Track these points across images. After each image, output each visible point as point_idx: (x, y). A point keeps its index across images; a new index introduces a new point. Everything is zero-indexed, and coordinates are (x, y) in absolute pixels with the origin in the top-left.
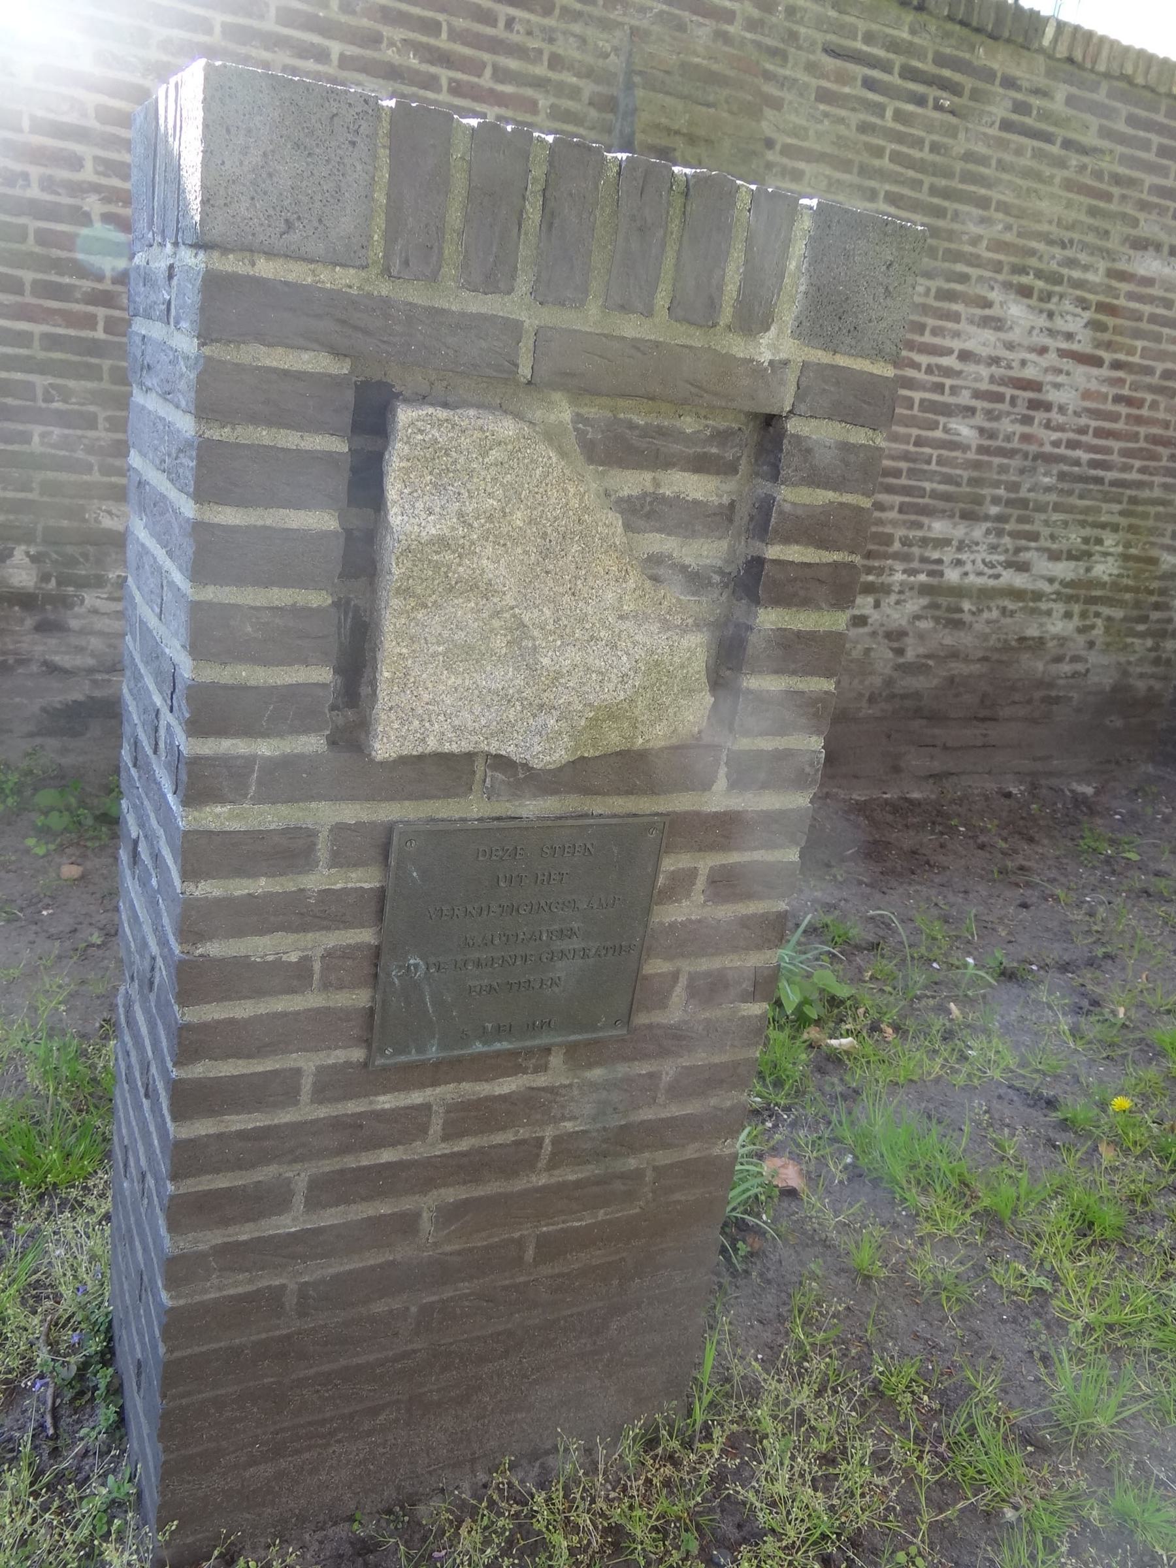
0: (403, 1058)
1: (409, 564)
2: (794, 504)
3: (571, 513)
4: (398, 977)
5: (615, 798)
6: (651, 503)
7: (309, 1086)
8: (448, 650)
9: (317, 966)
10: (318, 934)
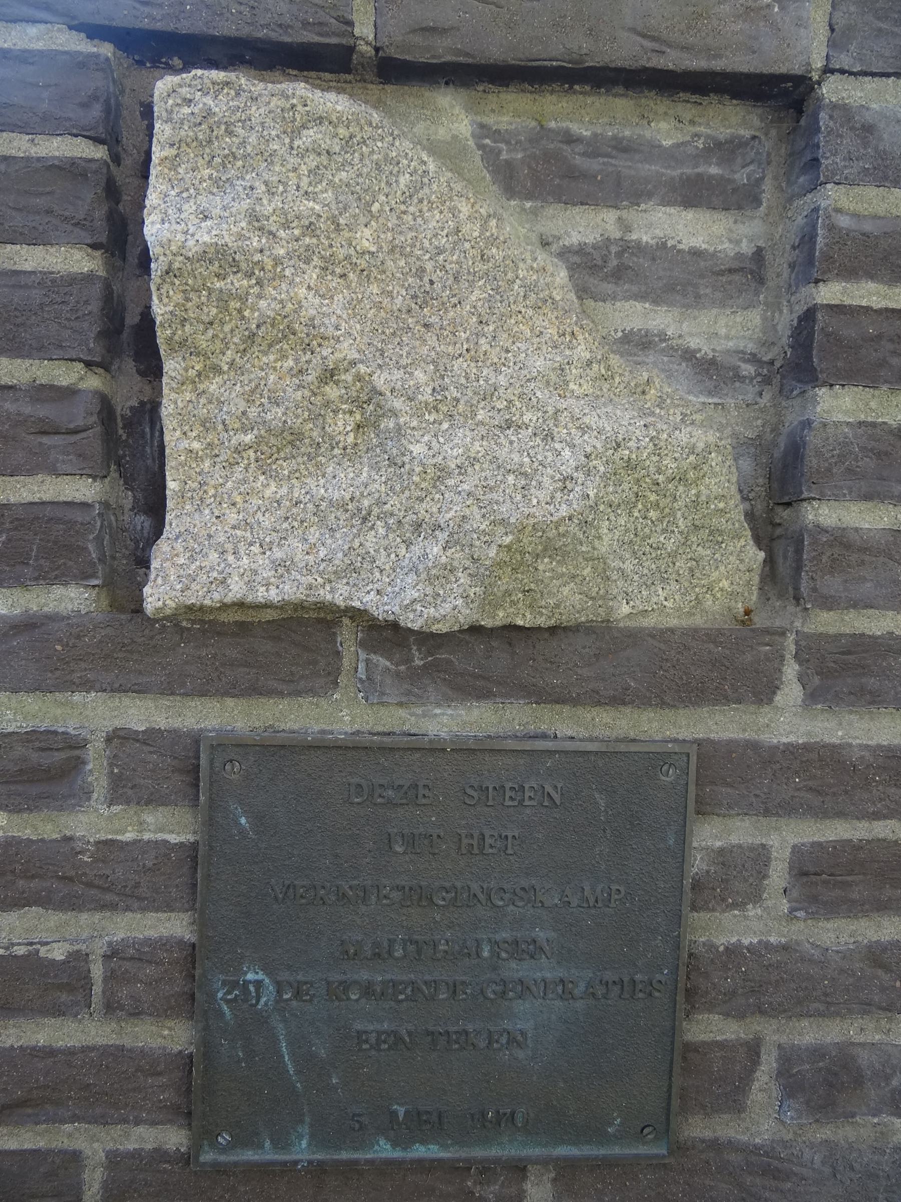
0: (249, 1155)
1: (178, 298)
2: (855, 215)
3: (467, 245)
4: (228, 1002)
5: (595, 711)
6: (620, 255)
7: (96, 1186)
8: (259, 439)
9: (97, 971)
10: (98, 916)
